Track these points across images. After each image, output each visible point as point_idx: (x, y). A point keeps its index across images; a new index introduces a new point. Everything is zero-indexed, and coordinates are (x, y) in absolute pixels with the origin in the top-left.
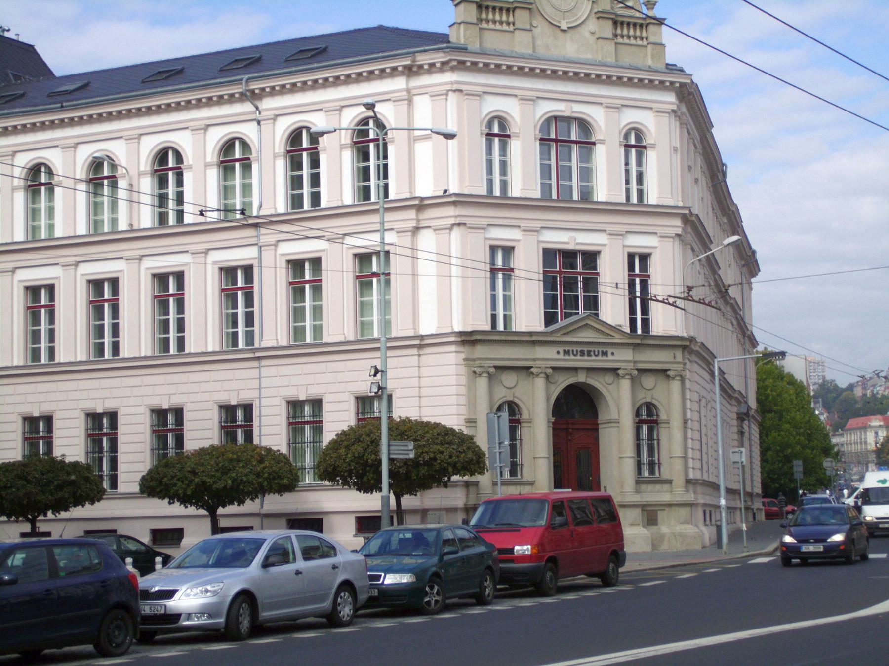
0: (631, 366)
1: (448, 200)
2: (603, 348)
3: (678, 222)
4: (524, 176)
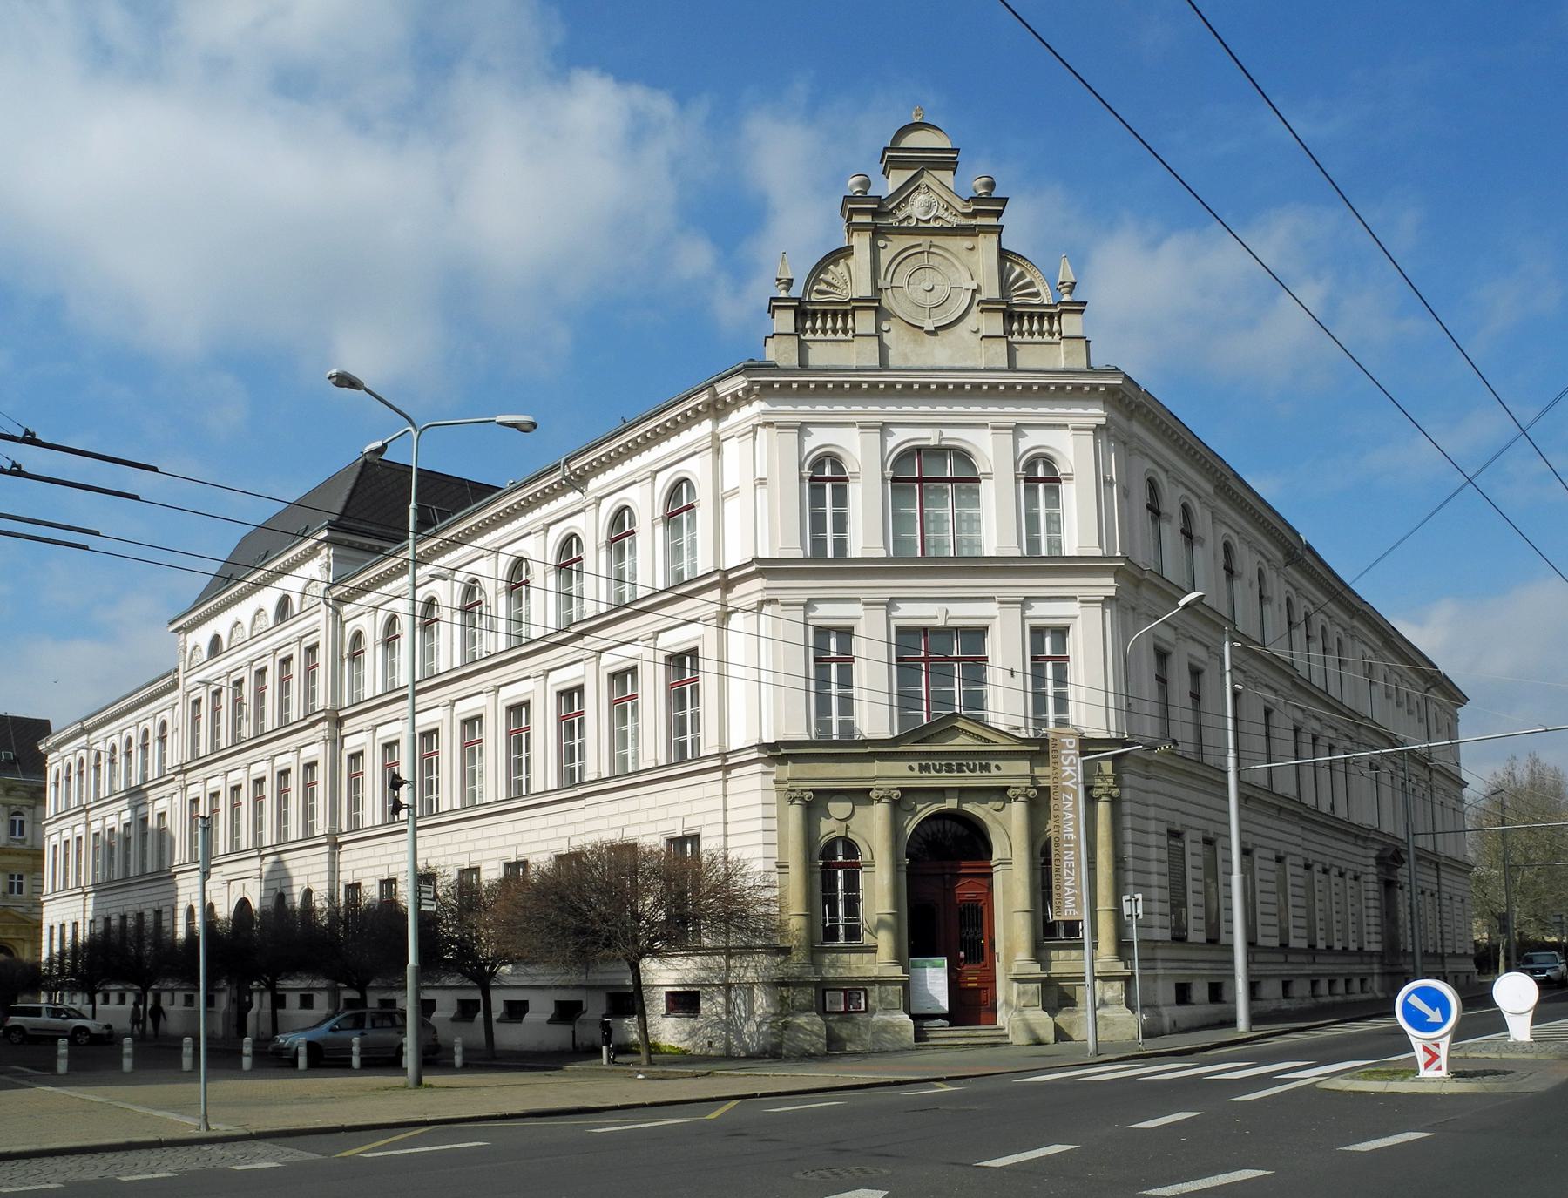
0: (1027, 782)
1: (767, 568)
2: (983, 759)
4: (865, 527)
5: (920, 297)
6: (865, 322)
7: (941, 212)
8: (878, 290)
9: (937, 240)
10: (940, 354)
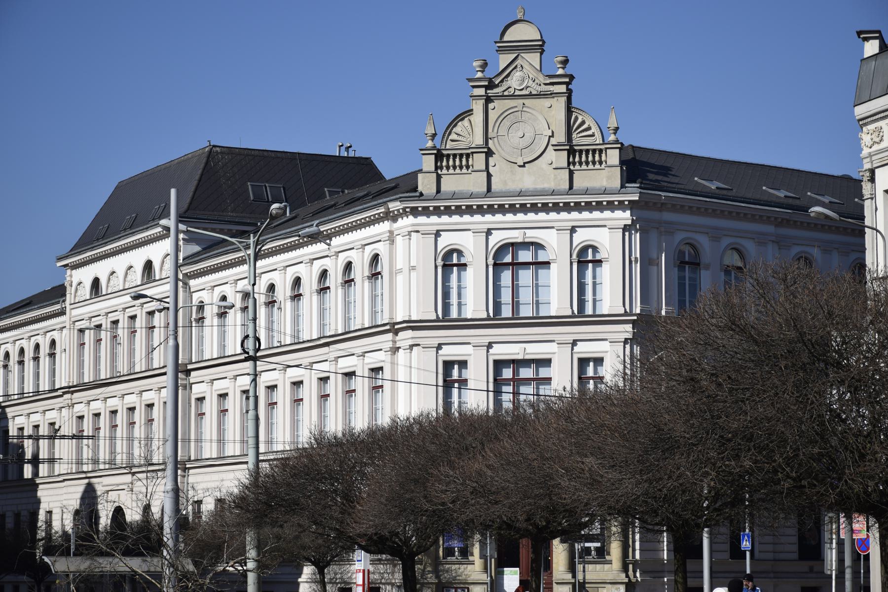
8: (487, 139)
9: (527, 102)
10: (527, 180)
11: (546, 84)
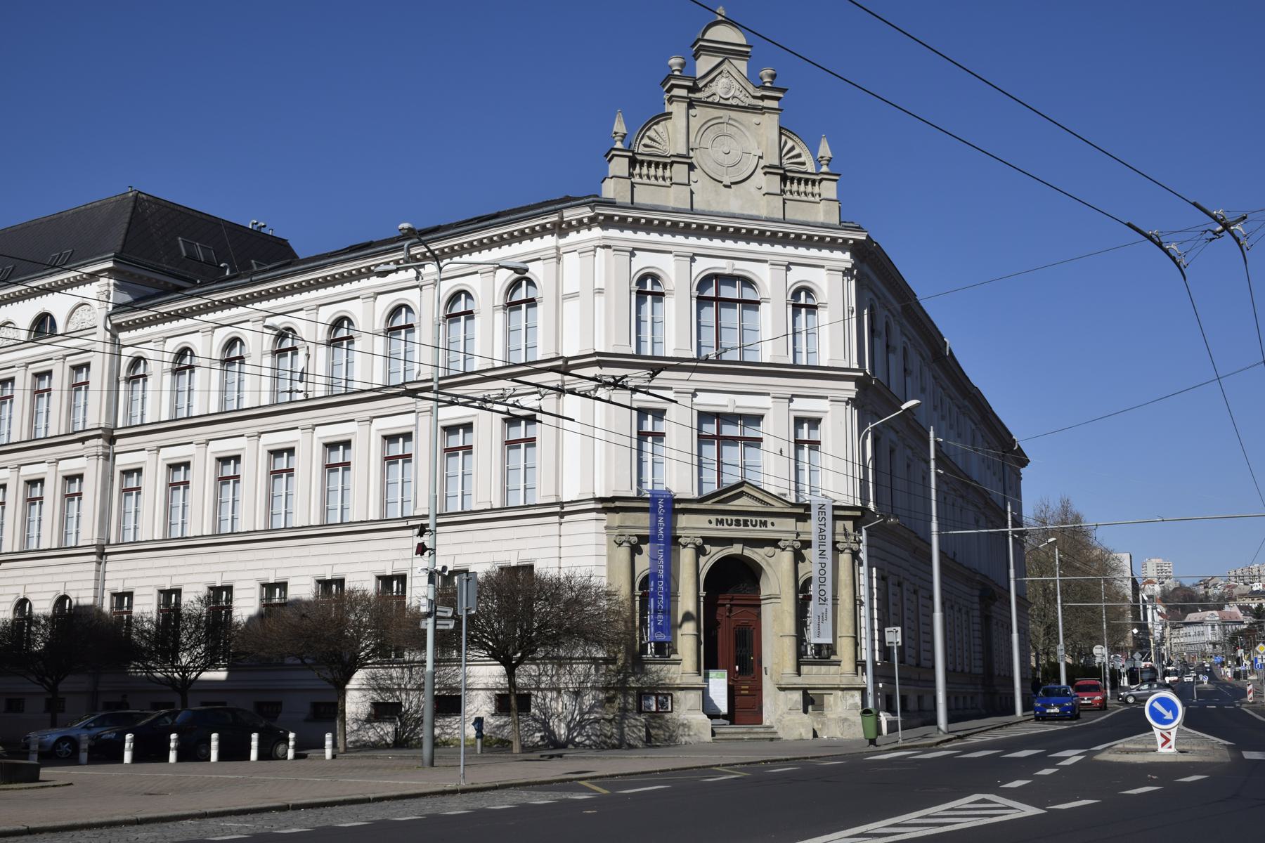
3: (852, 385)
5: (721, 158)
6: (680, 172)
7: (737, 94)
8: (689, 149)
9: (733, 114)
10: (733, 203)
11: (754, 97)
